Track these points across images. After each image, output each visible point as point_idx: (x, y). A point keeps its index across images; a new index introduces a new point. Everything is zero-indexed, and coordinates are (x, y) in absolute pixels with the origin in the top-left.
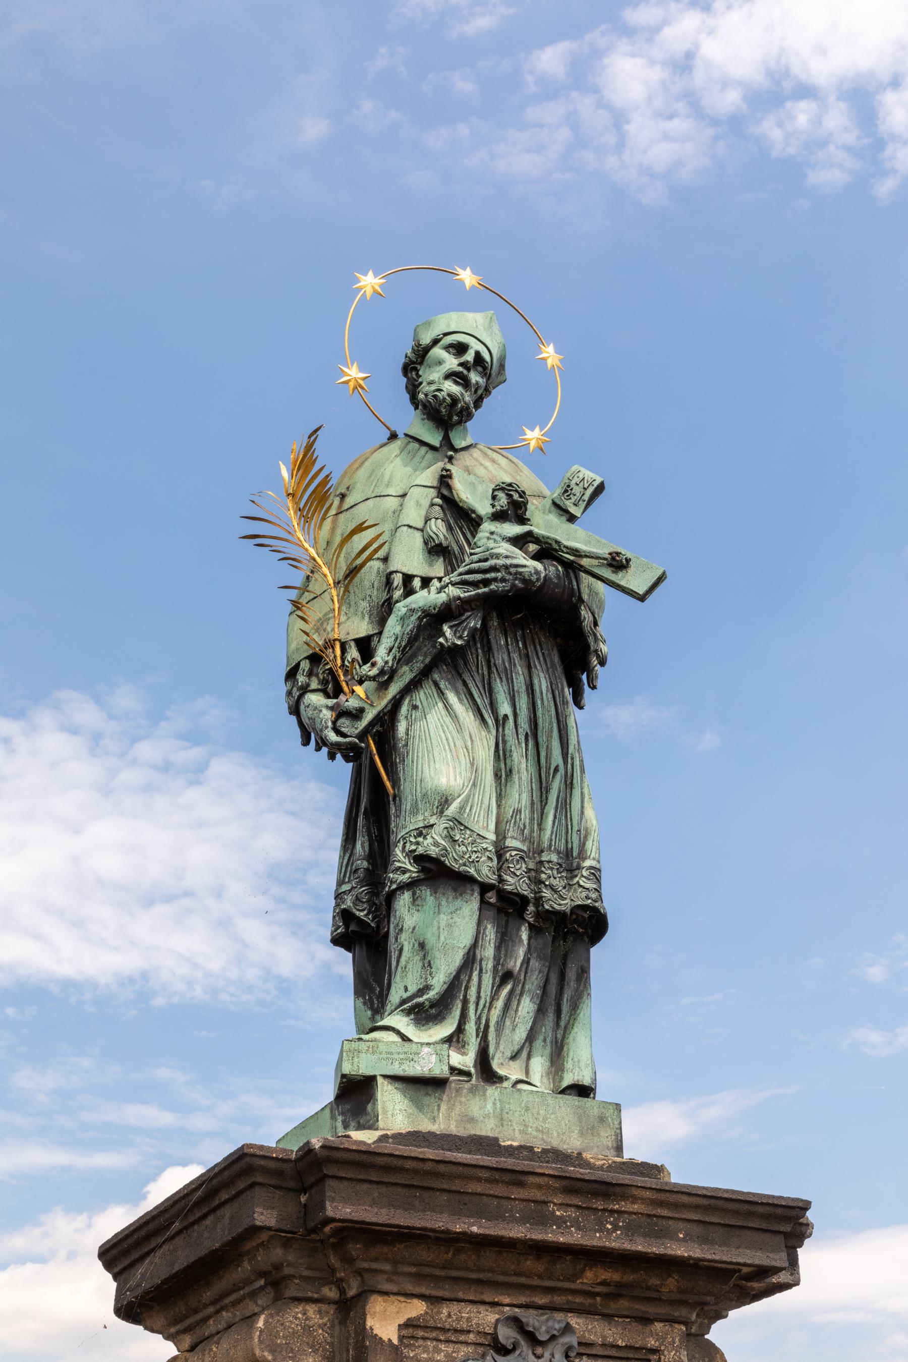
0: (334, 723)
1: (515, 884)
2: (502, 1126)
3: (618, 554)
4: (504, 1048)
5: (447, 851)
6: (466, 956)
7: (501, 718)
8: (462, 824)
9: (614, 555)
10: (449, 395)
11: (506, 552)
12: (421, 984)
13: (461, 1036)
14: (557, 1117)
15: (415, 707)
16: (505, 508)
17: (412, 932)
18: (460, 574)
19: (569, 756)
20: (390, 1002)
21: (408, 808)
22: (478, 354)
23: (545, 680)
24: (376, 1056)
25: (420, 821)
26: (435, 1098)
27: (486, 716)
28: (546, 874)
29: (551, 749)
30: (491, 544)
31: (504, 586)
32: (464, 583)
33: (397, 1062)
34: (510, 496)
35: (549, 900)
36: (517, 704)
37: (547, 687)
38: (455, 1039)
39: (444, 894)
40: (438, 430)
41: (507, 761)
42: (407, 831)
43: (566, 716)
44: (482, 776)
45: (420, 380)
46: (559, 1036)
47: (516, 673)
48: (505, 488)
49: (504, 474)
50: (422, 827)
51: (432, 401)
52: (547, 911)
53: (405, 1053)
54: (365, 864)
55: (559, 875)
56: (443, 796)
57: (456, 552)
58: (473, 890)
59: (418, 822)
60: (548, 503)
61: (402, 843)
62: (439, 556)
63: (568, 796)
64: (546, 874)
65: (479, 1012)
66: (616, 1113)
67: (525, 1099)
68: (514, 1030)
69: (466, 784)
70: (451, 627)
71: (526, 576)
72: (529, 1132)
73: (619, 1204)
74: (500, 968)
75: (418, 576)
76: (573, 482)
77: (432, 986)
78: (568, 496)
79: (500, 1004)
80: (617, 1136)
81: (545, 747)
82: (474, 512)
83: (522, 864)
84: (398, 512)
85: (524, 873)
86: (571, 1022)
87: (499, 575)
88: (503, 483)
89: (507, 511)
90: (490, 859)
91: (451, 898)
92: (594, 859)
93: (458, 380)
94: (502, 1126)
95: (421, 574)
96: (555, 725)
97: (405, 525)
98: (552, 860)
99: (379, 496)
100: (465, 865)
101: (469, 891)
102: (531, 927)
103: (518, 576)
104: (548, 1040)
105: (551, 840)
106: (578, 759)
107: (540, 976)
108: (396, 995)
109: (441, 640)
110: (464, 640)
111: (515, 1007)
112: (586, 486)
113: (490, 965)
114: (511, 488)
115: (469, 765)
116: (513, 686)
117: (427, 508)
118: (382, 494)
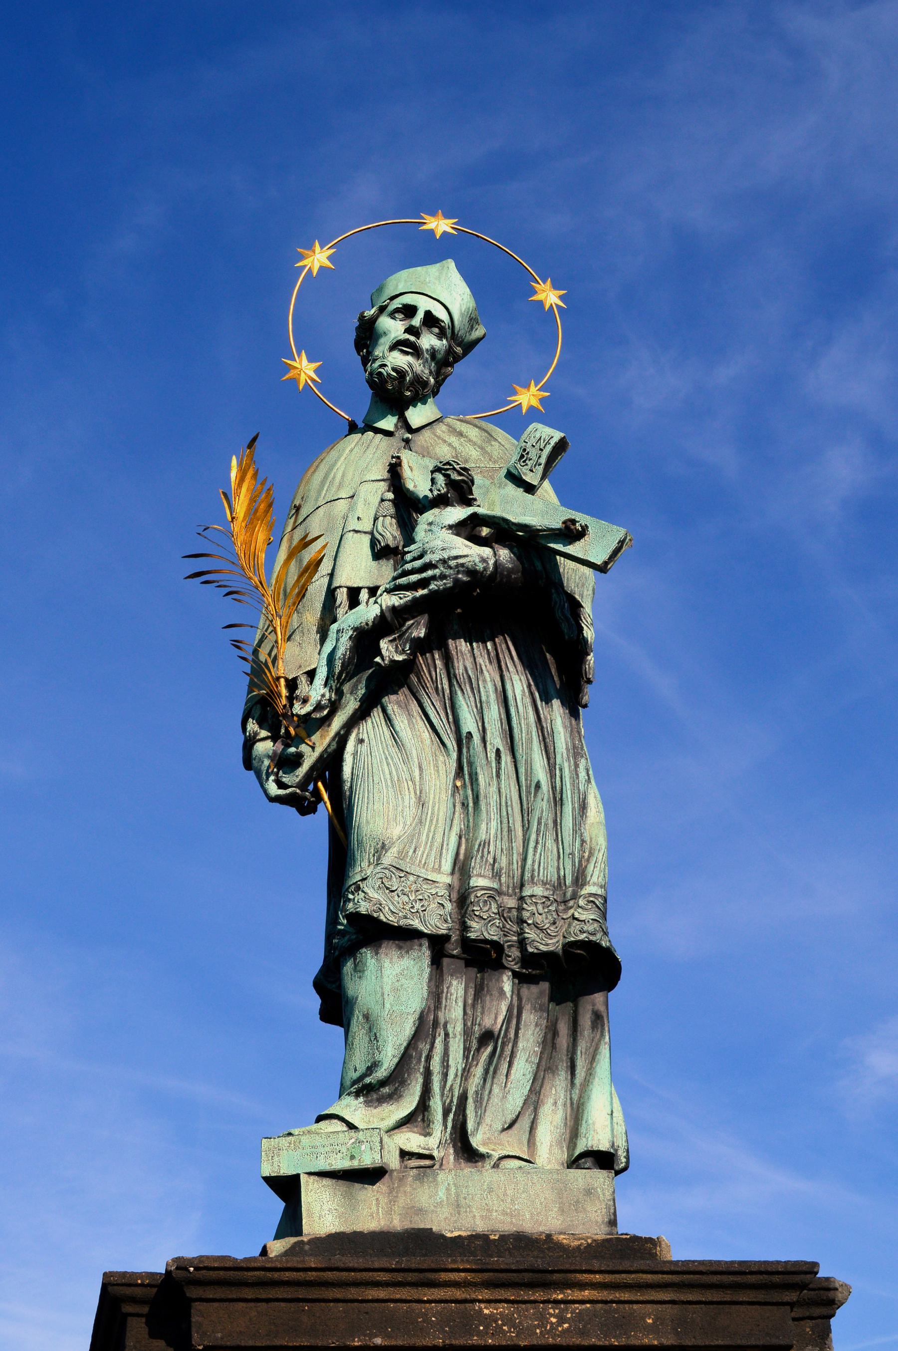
2: (459, 1214)
3: (574, 522)
4: (492, 1121)
5: (381, 905)
6: (417, 1023)
8: (402, 871)
9: (569, 523)
10: (394, 369)
12: (369, 1060)
13: (426, 1113)
15: (361, 741)
16: (443, 492)
19: (557, 767)
22: (428, 314)
23: (519, 682)
26: (373, 1192)
31: (445, 584)
34: (447, 476)
35: (534, 941)
40: (392, 410)
44: (433, 809)
49: (471, 448)
50: (359, 881)
52: (532, 953)
55: (546, 910)
58: (421, 945)
63: (559, 815)
68: (504, 1097)
69: (408, 823)
72: (494, 1217)
73: (564, 1293)
74: (476, 1029)
75: (364, 588)
76: (529, 445)
77: (379, 1062)
78: (524, 462)
79: (478, 1071)
80: (610, 1209)
83: (490, 904)
85: (493, 915)
87: (437, 572)
89: (446, 494)
92: (594, 884)
94: (459, 1214)
96: (534, 734)
97: (350, 531)
98: (535, 893)
99: (330, 502)
100: (405, 917)
102: (515, 975)
103: (461, 569)
104: (560, 1103)
105: (533, 871)
107: (538, 1029)
109: (378, 659)
111: (505, 1072)
113: (459, 1028)
114: (448, 467)
115: (413, 800)
116: (480, 697)
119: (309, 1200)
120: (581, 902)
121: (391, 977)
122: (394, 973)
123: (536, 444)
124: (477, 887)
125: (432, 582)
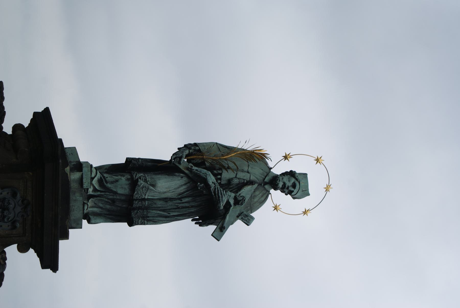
0: (178, 157)
1: (136, 203)
2: (74, 201)
3: (224, 229)
5: (140, 186)
7: (181, 199)
8: (148, 190)
10: (278, 184)
15: (182, 177)
17: (120, 179)
18: (218, 188)
22: (293, 191)
27: (181, 196)
30: (226, 196)
32: (215, 189)
34: (241, 200)
36: (186, 203)
38: (95, 190)
45: (286, 175)
46: (103, 215)
53: (88, 178)
57: (230, 187)
59: (148, 179)
60: (243, 211)
61: (143, 175)
65: (104, 195)
68: (101, 203)
70: (203, 186)
79: (106, 200)
81: (175, 211)
82: (240, 191)
84: (243, 171)
88: (245, 199)
90: (140, 197)
95: (222, 178)
97: (237, 173)
100: (137, 191)
104: (102, 212)
106: (173, 219)
108: (106, 175)
109: (199, 183)
110: (200, 189)
112: (247, 221)
115: (165, 191)
116: (191, 202)
118: (249, 166)
120: (143, 221)
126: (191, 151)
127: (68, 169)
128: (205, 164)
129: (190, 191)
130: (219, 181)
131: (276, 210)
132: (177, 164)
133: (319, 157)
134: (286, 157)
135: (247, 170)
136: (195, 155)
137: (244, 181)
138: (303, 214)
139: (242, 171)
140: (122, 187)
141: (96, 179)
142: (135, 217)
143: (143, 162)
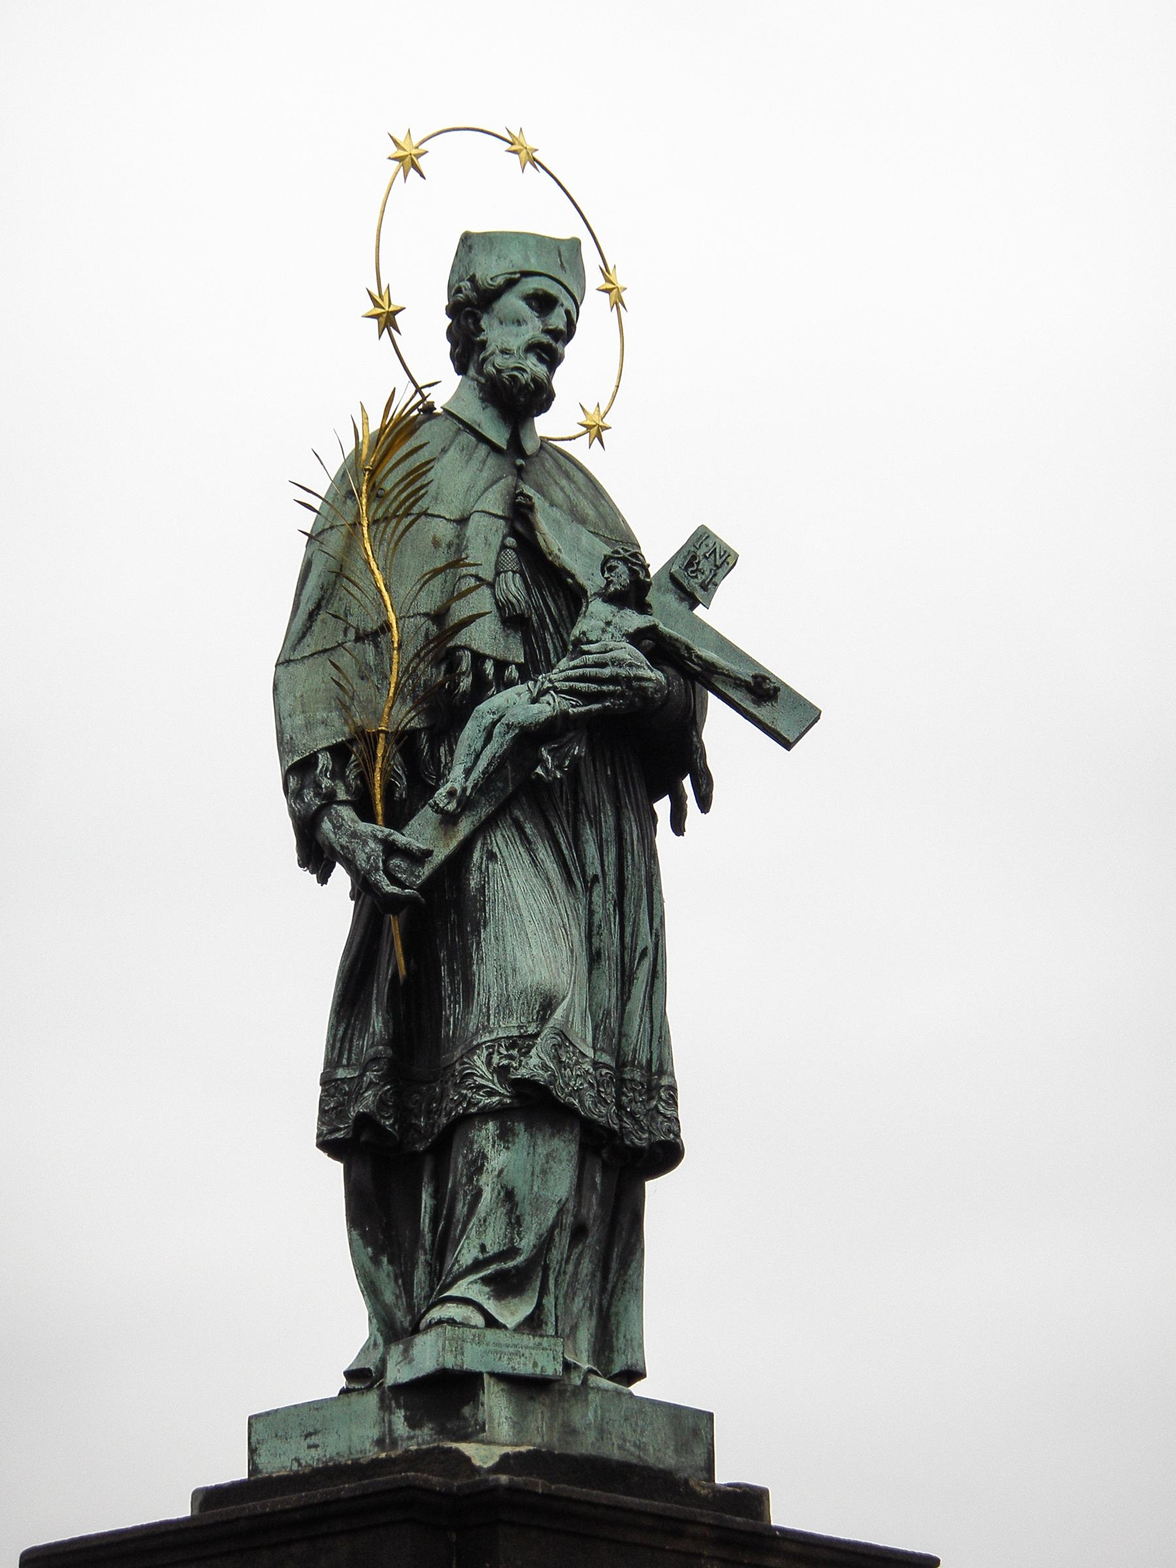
0: (384, 862)
2: (602, 1438)
3: (764, 678)
5: (555, 1076)
11: (629, 657)
12: (505, 1245)
14: (653, 1429)
15: (492, 856)
17: (499, 1175)
18: (567, 679)
19: (654, 931)
20: (459, 1261)
21: (493, 1003)
24: (483, 1348)
25: (514, 1027)
28: (627, 1097)
29: (639, 924)
30: (612, 644)
31: (621, 704)
32: (571, 692)
33: (506, 1357)
34: (633, 573)
35: (631, 1132)
36: (605, 858)
37: (638, 835)
39: (540, 1131)
41: (593, 940)
42: (493, 1037)
43: (652, 876)
45: (482, 337)
47: (604, 815)
48: (628, 559)
50: (516, 1036)
51: (507, 383)
52: (627, 1147)
54: (390, 1052)
56: (547, 998)
59: (507, 1027)
61: (485, 1053)
62: (516, 631)
64: (627, 1097)
66: (709, 1426)
67: (625, 1406)
68: (573, 1299)
70: (549, 752)
71: (649, 693)
77: (520, 1249)
78: (692, 572)
82: (573, 577)
86: (619, 1286)
90: (591, 1085)
91: (547, 1135)
93: (544, 355)
97: (472, 575)
101: (568, 1129)
104: (595, 1307)
108: (467, 1254)
115: (569, 954)
116: (601, 832)
117: (498, 550)
118: (429, 512)
119: (492, 1404)
121: (542, 1156)
122: (545, 1152)
123: (710, 555)
124: (601, 1063)
125: (609, 698)
126: (342, 795)
127: (480, 1455)
128: (413, 734)
129: (557, 829)
130: (513, 672)
131: (604, 434)
132: (426, 871)
133: (393, 151)
134: (388, 321)
135: (450, 526)
136: (365, 778)
137: (510, 548)
138: (618, 308)
139: (453, 549)
140: (544, 1172)
141: (491, 1306)
142: (651, 1133)
143: (349, 1059)
